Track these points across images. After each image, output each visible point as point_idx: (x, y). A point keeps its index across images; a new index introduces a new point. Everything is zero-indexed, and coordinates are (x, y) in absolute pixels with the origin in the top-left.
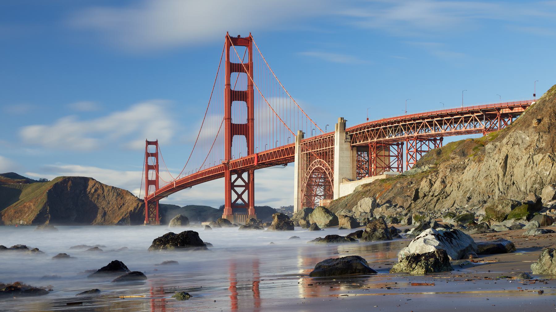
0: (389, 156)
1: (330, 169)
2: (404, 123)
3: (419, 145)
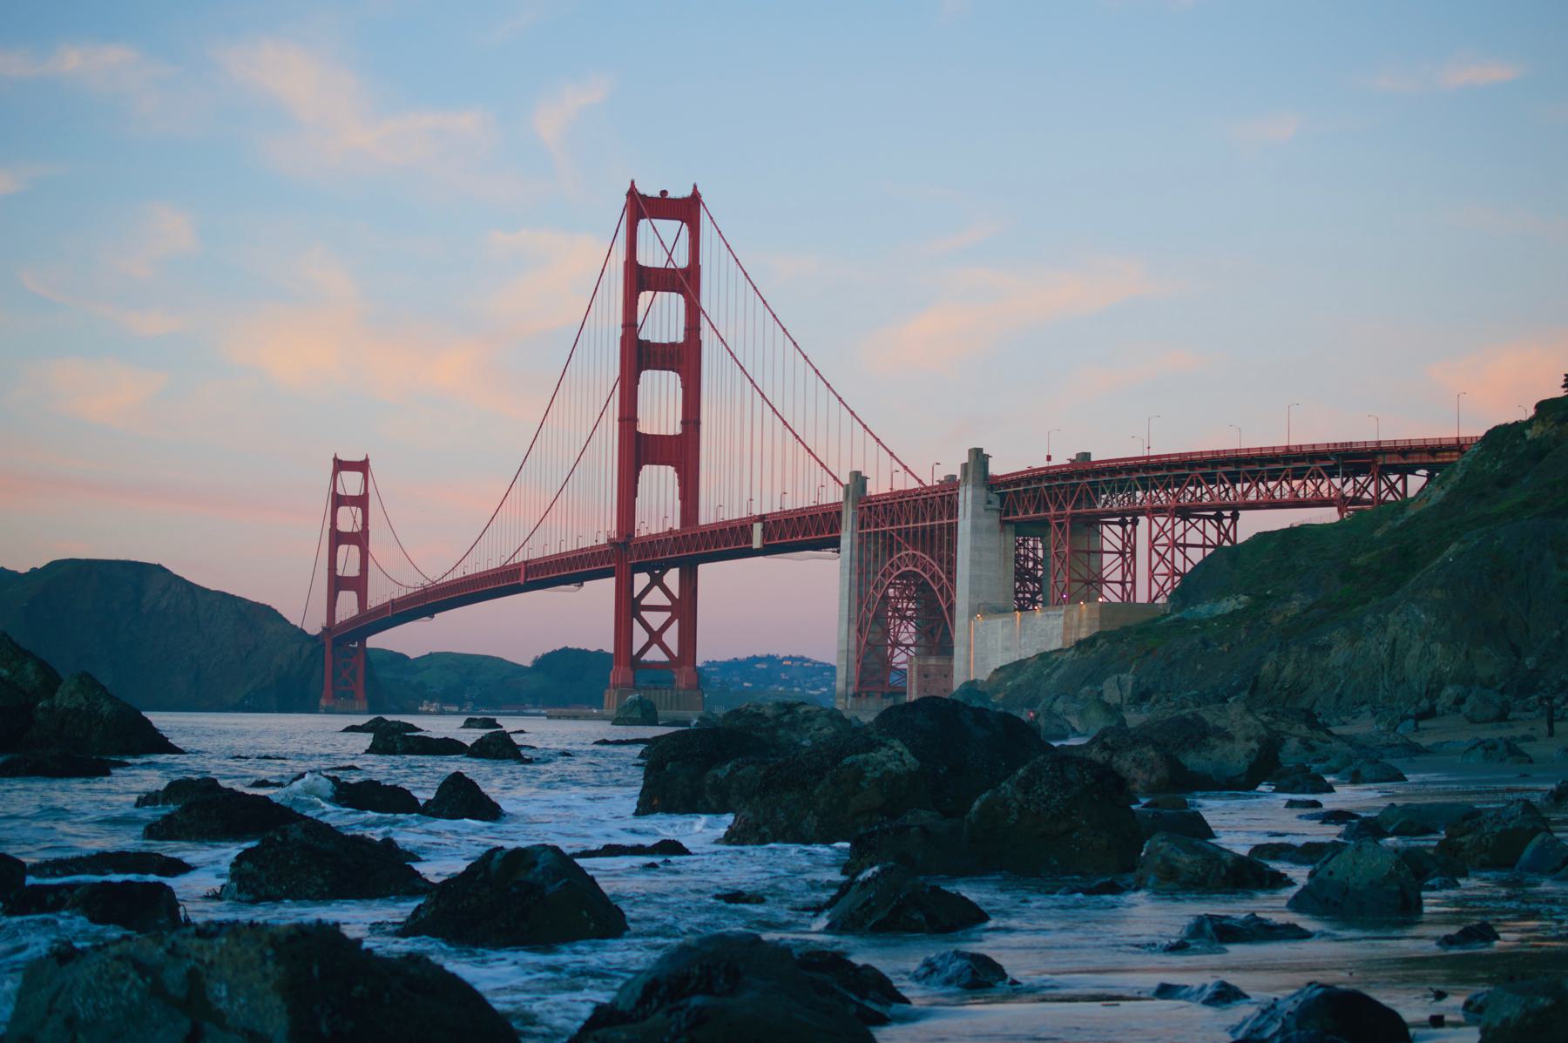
0: (1102, 552)
1: (944, 577)
2: (1144, 475)
3: (1179, 529)
